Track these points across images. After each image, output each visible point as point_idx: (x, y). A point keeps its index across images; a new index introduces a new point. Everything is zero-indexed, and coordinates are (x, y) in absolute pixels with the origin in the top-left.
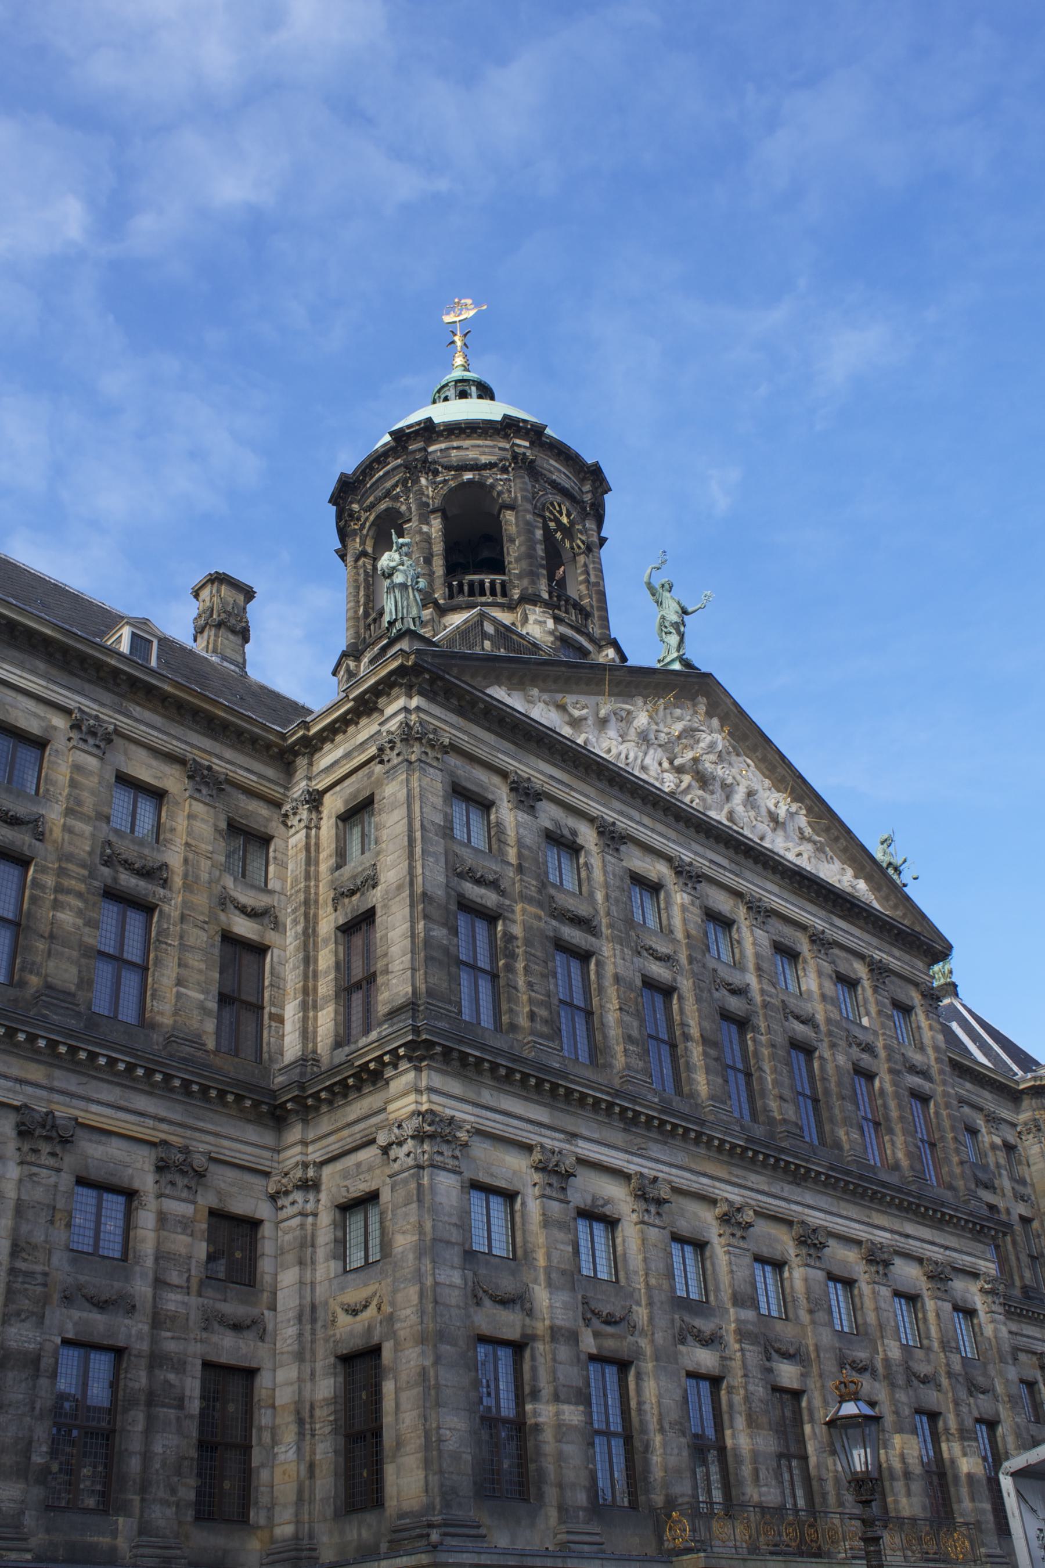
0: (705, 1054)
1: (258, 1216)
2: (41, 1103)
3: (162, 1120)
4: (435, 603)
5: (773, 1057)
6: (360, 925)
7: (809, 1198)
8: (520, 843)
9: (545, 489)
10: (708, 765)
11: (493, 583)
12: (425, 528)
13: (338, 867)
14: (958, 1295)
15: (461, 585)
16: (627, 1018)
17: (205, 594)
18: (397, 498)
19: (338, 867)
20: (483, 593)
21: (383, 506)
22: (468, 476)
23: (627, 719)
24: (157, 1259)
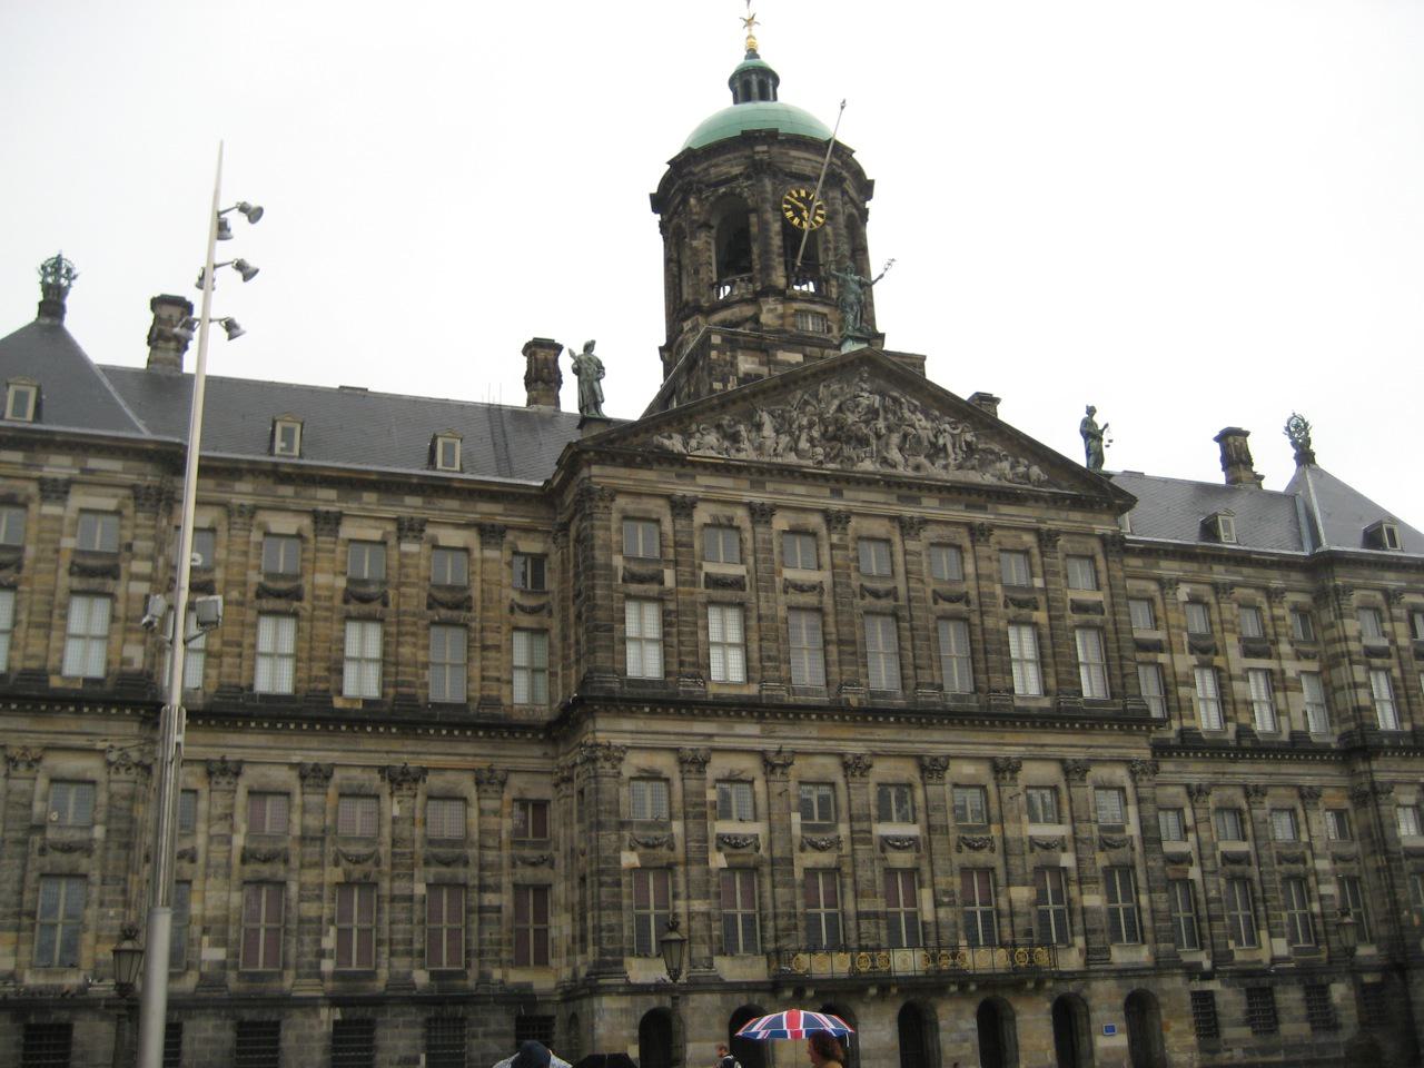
0: (840, 653)
1: (546, 798)
2: (396, 761)
3: (476, 755)
7: (937, 736)
8: (677, 544)
9: (783, 182)
22: (722, 190)
24: (481, 832)
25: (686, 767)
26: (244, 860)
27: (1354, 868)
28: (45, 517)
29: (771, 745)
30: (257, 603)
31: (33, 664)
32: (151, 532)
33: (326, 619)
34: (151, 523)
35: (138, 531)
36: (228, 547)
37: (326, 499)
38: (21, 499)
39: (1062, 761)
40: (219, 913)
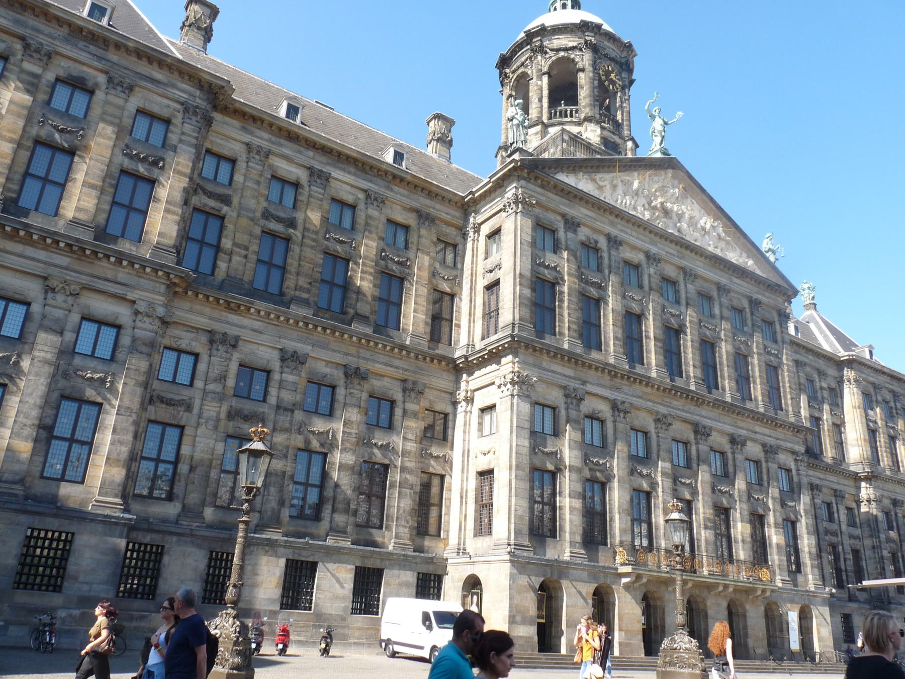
0: (655, 345)
2: (353, 362)
4: (543, 123)
5: (692, 346)
6: (493, 286)
7: (704, 413)
10: (669, 205)
11: (571, 111)
12: (539, 83)
13: (486, 258)
14: (782, 461)
15: (556, 113)
16: (616, 329)
17: (432, 124)
18: (526, 67)
19: (486, 258)
20: (566, 116)
21: (520, 71)
22: (562, 54)
23: (630, 184)
25: (570, 400)
26: (231, 416)
27: (857, 544)
28: (107, 103)
29: (618, 396)
30: (263, 222)
31: (82, 216)
32: (194, 141)
33: (312, 247)
34: (196, 135)
35: (183, 137)
36: (245, 176)
37: (319, 163)
38: (90, 84)
39: (764, 445)
40: (206, 456)
